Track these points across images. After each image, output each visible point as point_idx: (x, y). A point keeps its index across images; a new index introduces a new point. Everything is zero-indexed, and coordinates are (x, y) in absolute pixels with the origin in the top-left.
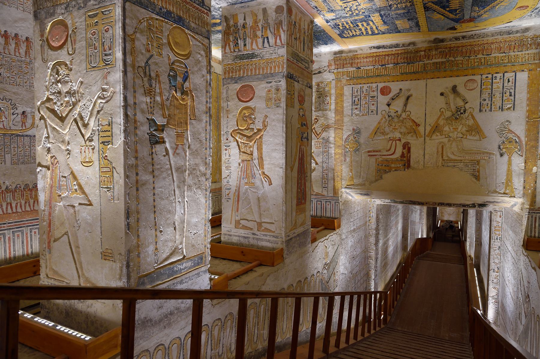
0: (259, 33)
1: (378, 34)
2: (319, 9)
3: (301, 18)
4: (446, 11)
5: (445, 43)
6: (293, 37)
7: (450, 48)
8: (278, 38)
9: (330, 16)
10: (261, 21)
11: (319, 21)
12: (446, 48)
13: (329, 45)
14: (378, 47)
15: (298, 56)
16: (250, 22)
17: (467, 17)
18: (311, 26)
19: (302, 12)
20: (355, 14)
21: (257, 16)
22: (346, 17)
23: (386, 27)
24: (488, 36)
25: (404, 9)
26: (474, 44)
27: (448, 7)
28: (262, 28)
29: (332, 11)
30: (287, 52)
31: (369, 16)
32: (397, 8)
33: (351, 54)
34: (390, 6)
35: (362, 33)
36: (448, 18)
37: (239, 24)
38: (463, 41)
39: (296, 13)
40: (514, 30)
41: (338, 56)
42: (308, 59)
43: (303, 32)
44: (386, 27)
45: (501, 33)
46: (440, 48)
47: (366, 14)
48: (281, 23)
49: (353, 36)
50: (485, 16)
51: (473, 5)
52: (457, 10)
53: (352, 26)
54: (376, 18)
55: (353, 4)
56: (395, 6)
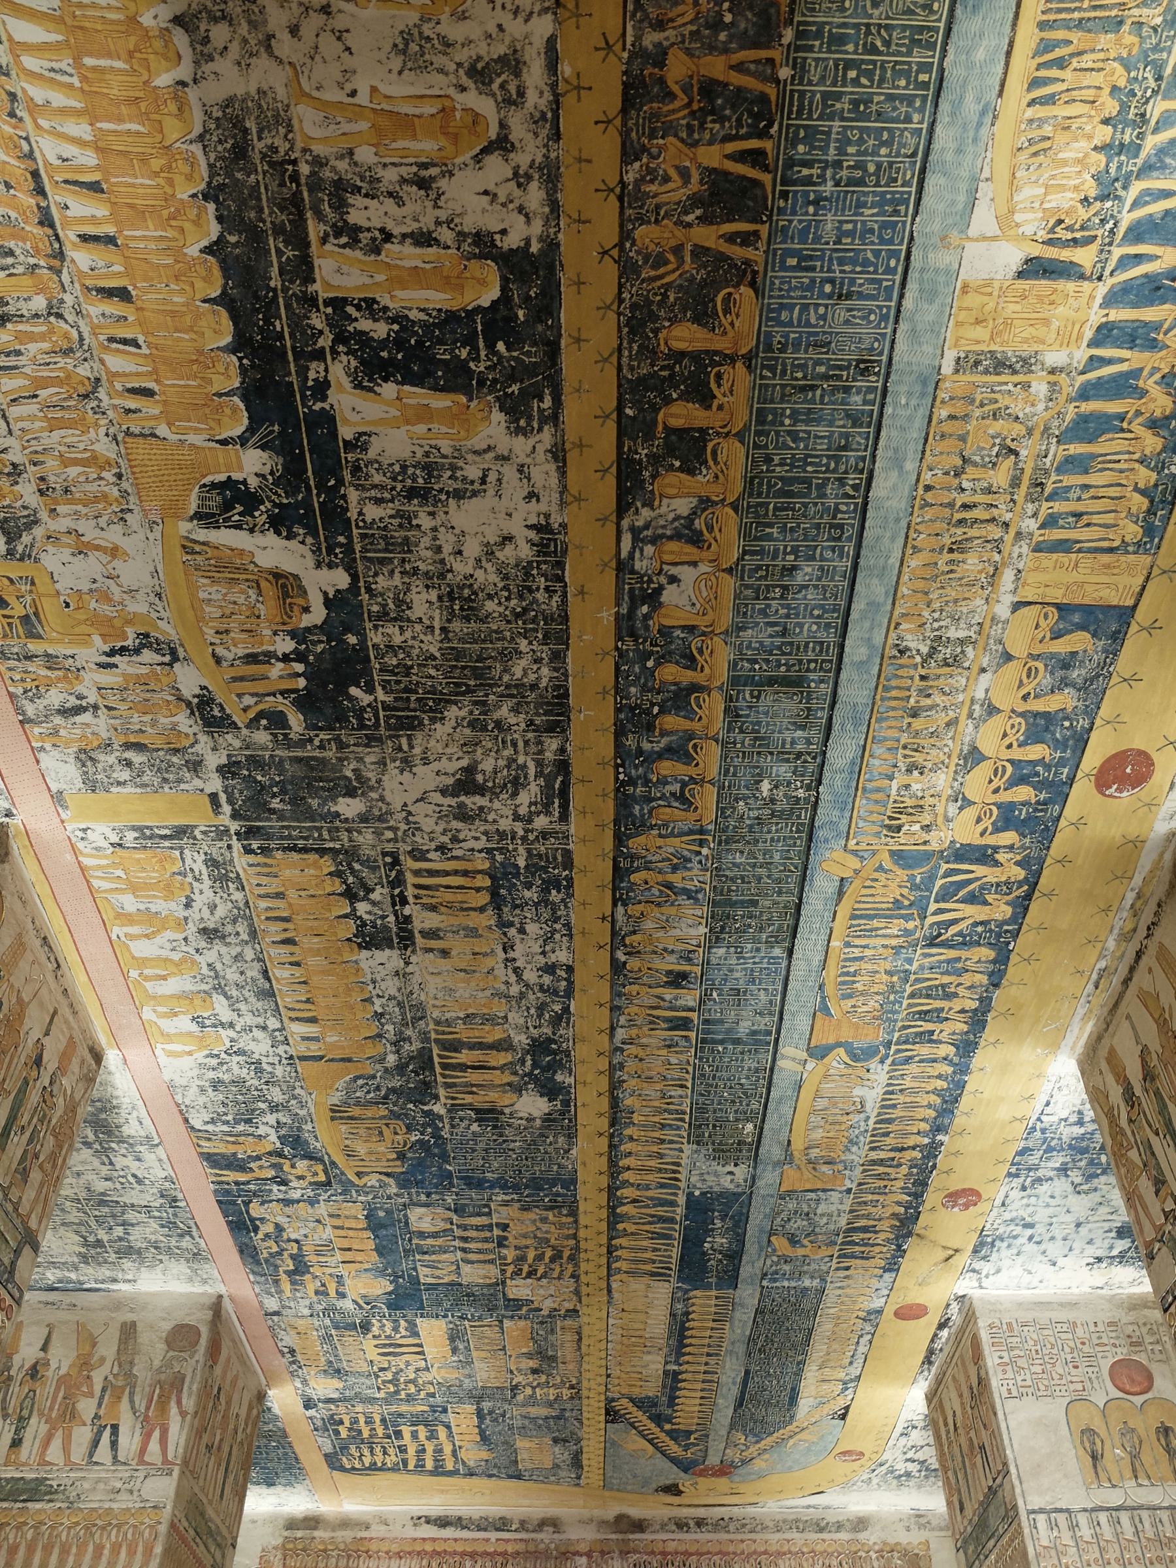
0: (87, 1407)
1: (454, 1473)
2: (299, 1357)
3: (236, 1377)
4: (662, 1430)
5: (647, 1536)
6: (205, 1438)
7: (664, 1554)
8: (157, 1434)
9: (324, 1387)
10: (108, 1364)
11: (283, 1399)
12: (653, 1553)
13: (279, 1489)
14: (443, 1522)
15: (202, 1514)
16: (61, 1359)
17: (713, 1460)
18: (255, 1412)
19: (243, 1359)
20: (403, 1395)
21: (94, 1345)
22: (372, 1400)
23: (485, 1455)
24: (765, 1528)
25: (550, 1404)
26: (731, 1549)
27: (669, 1420)
28: (104, 1390)
29: (338, 1371)
30: (177, 1494)
31: (445, 1411)
32: (532, 1401)
33: (347, 1535)
34: (514, 1388)
35: (405, 1463)
36: (663, 1453)
37: (17, 1360)
38: (699, 1536)
39: (228, 1360)
40: (831, 1518)
41: (299, 1534)
42: (225, 1532)
43: (231, 1427)
44: (485, 1455)
45: (798, 1524)
46: (635, 1551)
47: (439, 1400)
48: (178, 1382)
49: (373, 1467)
50: (759, 1464)
51: (732, 1426)
52: (690, 1433)
53: (380, 1431)
54: (463, 1420)
55: (408, 1364)
56: (529, 1391)
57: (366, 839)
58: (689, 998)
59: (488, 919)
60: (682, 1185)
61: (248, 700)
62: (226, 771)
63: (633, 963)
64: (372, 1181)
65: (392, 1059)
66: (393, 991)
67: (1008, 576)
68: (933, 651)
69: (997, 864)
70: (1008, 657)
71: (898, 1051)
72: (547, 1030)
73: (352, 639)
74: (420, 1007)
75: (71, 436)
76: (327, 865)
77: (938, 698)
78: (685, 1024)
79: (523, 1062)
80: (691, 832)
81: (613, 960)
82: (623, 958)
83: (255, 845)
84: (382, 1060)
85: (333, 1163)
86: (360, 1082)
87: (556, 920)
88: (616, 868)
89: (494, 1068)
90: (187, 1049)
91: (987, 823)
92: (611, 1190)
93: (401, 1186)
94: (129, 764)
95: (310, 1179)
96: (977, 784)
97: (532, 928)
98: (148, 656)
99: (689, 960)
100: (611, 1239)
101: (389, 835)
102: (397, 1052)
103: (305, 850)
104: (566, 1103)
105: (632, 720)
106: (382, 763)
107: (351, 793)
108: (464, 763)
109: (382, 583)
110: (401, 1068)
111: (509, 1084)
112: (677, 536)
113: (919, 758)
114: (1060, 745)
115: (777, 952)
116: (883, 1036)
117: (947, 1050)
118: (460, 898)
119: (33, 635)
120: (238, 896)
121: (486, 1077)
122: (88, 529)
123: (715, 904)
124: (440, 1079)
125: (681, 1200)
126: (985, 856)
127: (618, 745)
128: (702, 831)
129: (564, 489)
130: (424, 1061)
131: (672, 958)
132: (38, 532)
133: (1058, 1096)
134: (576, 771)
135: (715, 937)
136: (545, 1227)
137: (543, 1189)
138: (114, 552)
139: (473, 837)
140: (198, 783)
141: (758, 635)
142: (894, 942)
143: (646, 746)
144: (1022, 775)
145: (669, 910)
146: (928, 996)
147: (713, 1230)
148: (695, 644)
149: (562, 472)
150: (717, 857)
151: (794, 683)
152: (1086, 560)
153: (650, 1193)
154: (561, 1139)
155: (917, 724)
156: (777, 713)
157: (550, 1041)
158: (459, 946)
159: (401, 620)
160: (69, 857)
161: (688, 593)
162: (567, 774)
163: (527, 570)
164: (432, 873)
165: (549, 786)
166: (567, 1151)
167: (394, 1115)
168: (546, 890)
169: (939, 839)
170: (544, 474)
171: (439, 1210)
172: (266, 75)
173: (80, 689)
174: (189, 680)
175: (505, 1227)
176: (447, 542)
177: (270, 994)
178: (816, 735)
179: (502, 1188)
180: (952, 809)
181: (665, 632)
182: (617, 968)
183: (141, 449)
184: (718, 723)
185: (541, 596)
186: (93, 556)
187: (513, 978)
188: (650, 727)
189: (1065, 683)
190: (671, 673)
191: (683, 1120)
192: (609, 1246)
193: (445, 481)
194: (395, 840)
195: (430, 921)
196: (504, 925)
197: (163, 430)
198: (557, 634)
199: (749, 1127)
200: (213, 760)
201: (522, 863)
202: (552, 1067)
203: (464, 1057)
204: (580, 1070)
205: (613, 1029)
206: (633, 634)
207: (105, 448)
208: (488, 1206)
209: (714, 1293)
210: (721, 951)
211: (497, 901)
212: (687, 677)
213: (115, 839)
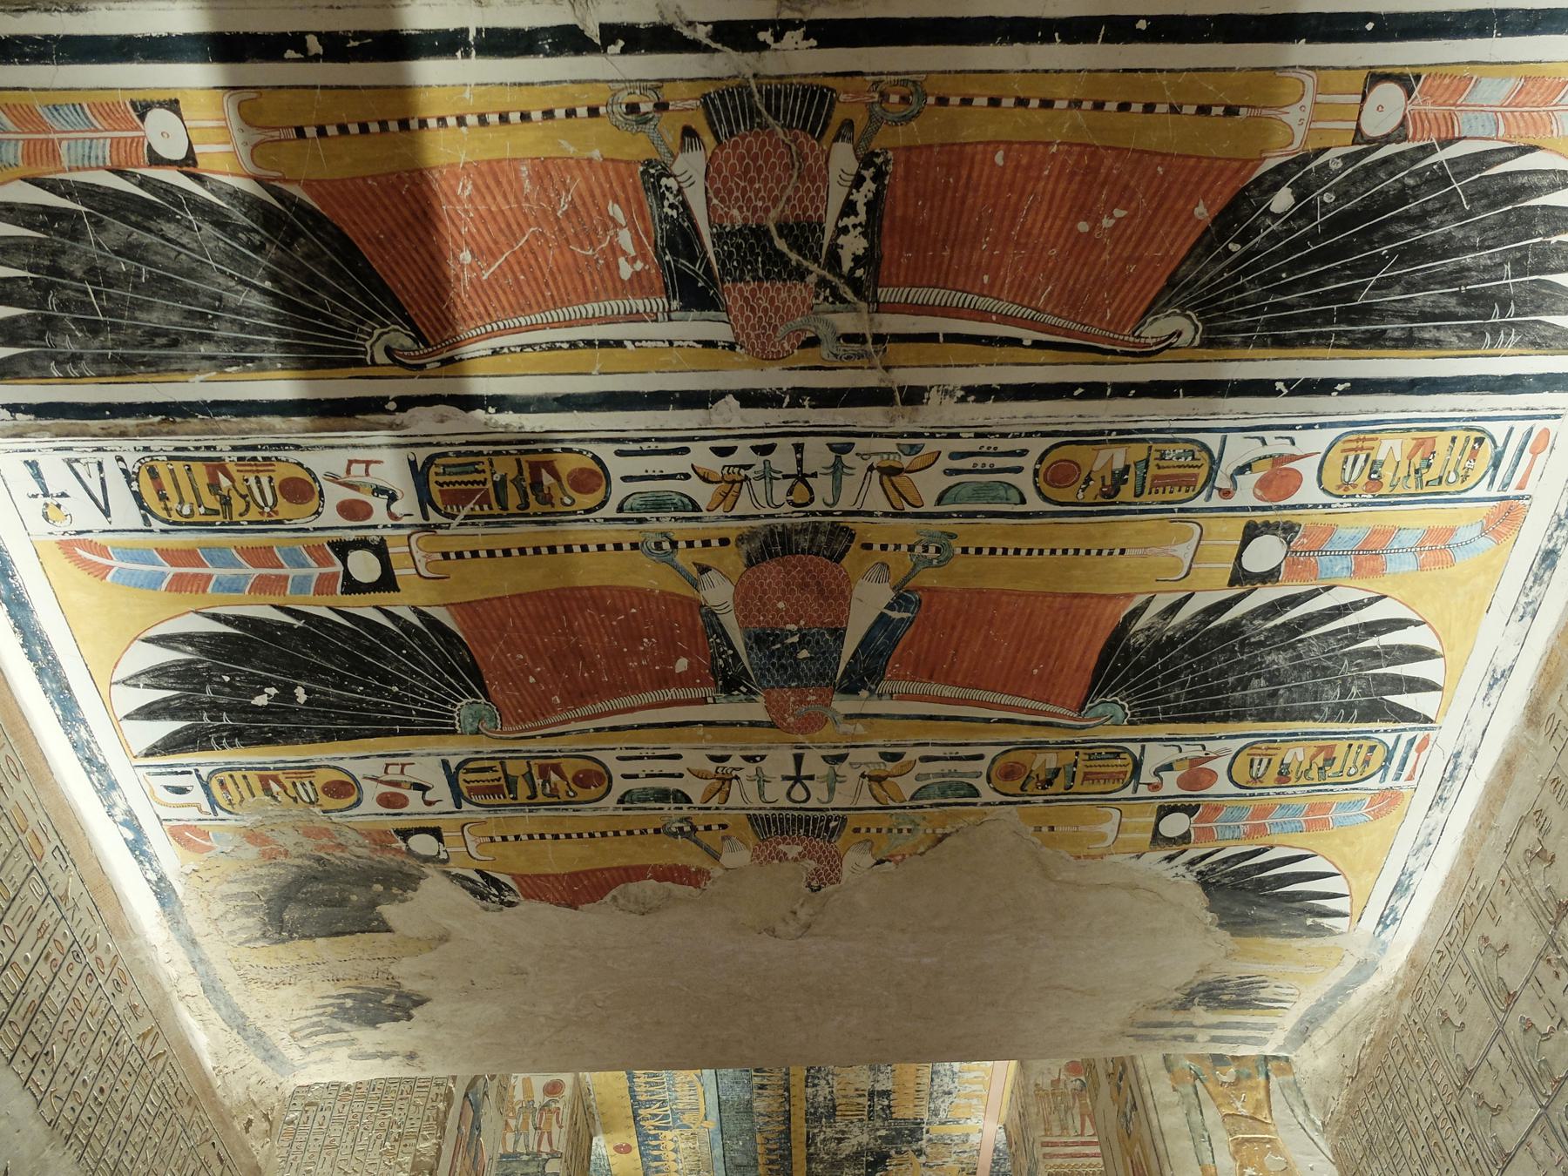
57: (879, 1123)
58: (756, 1081)
59: (837, 1102)
96: (671, 1146)
105: (787, 1157)
135: (749, 1102)
139: (840, 1126)
144: (657, 1147)
156: (741, 1159)
158: (852, 1093)
169: (677, 1132)
174: (923, 1159)
195: (860, 1100)
196: (832, 1100)
200: (923, 1143)
211: (834, 1107)
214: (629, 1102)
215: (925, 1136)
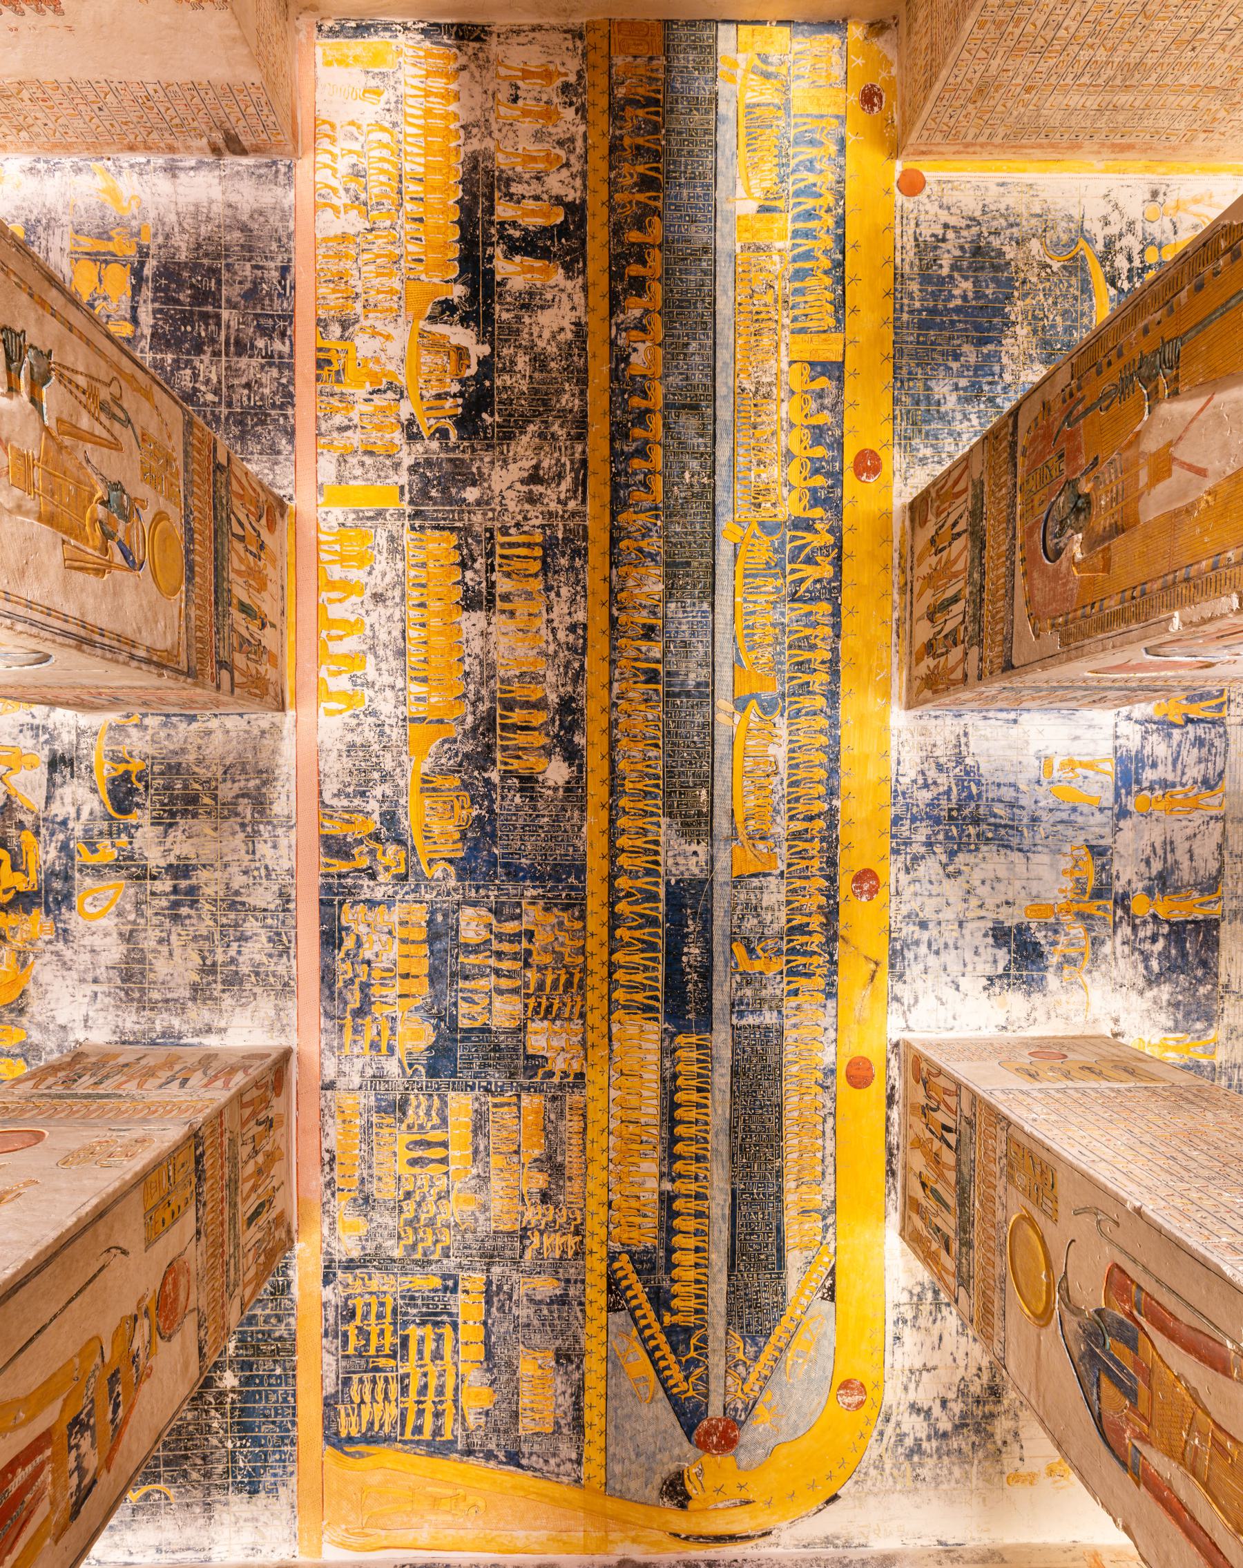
57: (477, 518)
59: (537, 585)
60: (662, 870)
61: (432, 421)
62: (413, 469)
63: (623, 618)
64: (438, 871)
65: (470, 719)
66: (478, 651)
67: (783, 347)
68: (757, 390)
69: (817, 532)
70: (793, 393)
71: (791, 703)
72: (570, 689)
73: (487, 383)
74: (492, 666)
75: (384, 280)
76: (454, 539)
77: (764, 418)
78: (652, 677)
79: (553, 720)
80: (651, 509)
81: (611, 615)
82: (616, 613)
83: (417, 523)
84: (463, 722)
85: (414, 848)
86: (446, 746)
87: (578, 582)
88: (612, 538)
89: (534, 729)
90: (341, 707)
91: (805, 501)
92: (612, 877)
93: (460, 878)
94: (363, 464)
95: (394, 871)
97: (564, 591)
98: (390, 395)
99: (655, 613)
100: (611, 953)
101: (490, 515)
102: (474, 713)
103: (443, 528)
104: (580, 768)
105: (619, 432)
106: (492, 462)
107: (474, 484)
108: (534, 462)
109: (505, 351)
110: (474, 729)
111: (543, 747)
112: (636, 328)
113: (761, 456)
114: (830, 447)
115: (706, 606)
116: (779, 688)
117: (820, 702)
118: (524, 566)
119: (338, 381)
120: (400, 565)
121: (529, 739)
122: (379, 326)
123: (667, 565)
124: (499, 742)
125: (662, 895)
126: (807, 525)
127: (612, 448)
128: (656, 508)
129: (587, 306)
130: (488, 723)
131: (645, 613)
132: (357, 326)
133: (903, 756)
134: (591, 466)
135: (669, 595)
136: (563, 937)
137: (560, 881)
138: (388, 337)
140: (396, 478)
141: (675, 380)
142: (772, 598)
143: (626, 449)
145: (642, 570)
146: (800, 647)
147: (687, 935)
148: (647, 384)
149: (586, 297)
150: (666, 527)
151: (695, 407)
152: (815, 337)
153: (639, 883)
154: (576, 813)
155: (757, 432)
156: (688, 424)
157: (572, 699)
158: (520, 606)
159: (511, 372)
160: (313, 533)
161: (642, 358)
162: (586, 468)
163: (569, 344)
164: (511, 545)
165: (577, 477)
166: (580, 829)
167: (466, 786)
168: (572, 558)
170: (579, 298)
171: (484, 912)
172: (489, 144)
173: (352, 415)
174: (406, 409)
175: (530, 935)
176: (535, 330)
177: (402, 653)
178: (708, 440)
179: (533, 879)
180: (785, 491)
181: (632, 378)
182: (613, 621)
183: (412, 284)
184: (661, 433)
185: (576, 358)
186: (379, 338)
187: (551, 638)
188: (627, 436)
189: (822, 407)
190: (636, 402)
191: (657, 786)
192: (611, 964)
193: (537, 301)
194: (492, 519)
196: (548, 588)
197: (423, 277)
198: (583, 382)
199: (704, 792)
200: (408, 461)
201: (560, 536)
202: (571, 728)
203: (517, 716)
204: (589, 728)
205: (611, 683)
206: (618, 379)
207: (397, 285)
208: (519, 905)
209: (694, 1039)
210: (672, 606)
211: (545, 568)
212: (644, 404)
213: (341, 520)
214: (847, 597)
215: (404, 478)
